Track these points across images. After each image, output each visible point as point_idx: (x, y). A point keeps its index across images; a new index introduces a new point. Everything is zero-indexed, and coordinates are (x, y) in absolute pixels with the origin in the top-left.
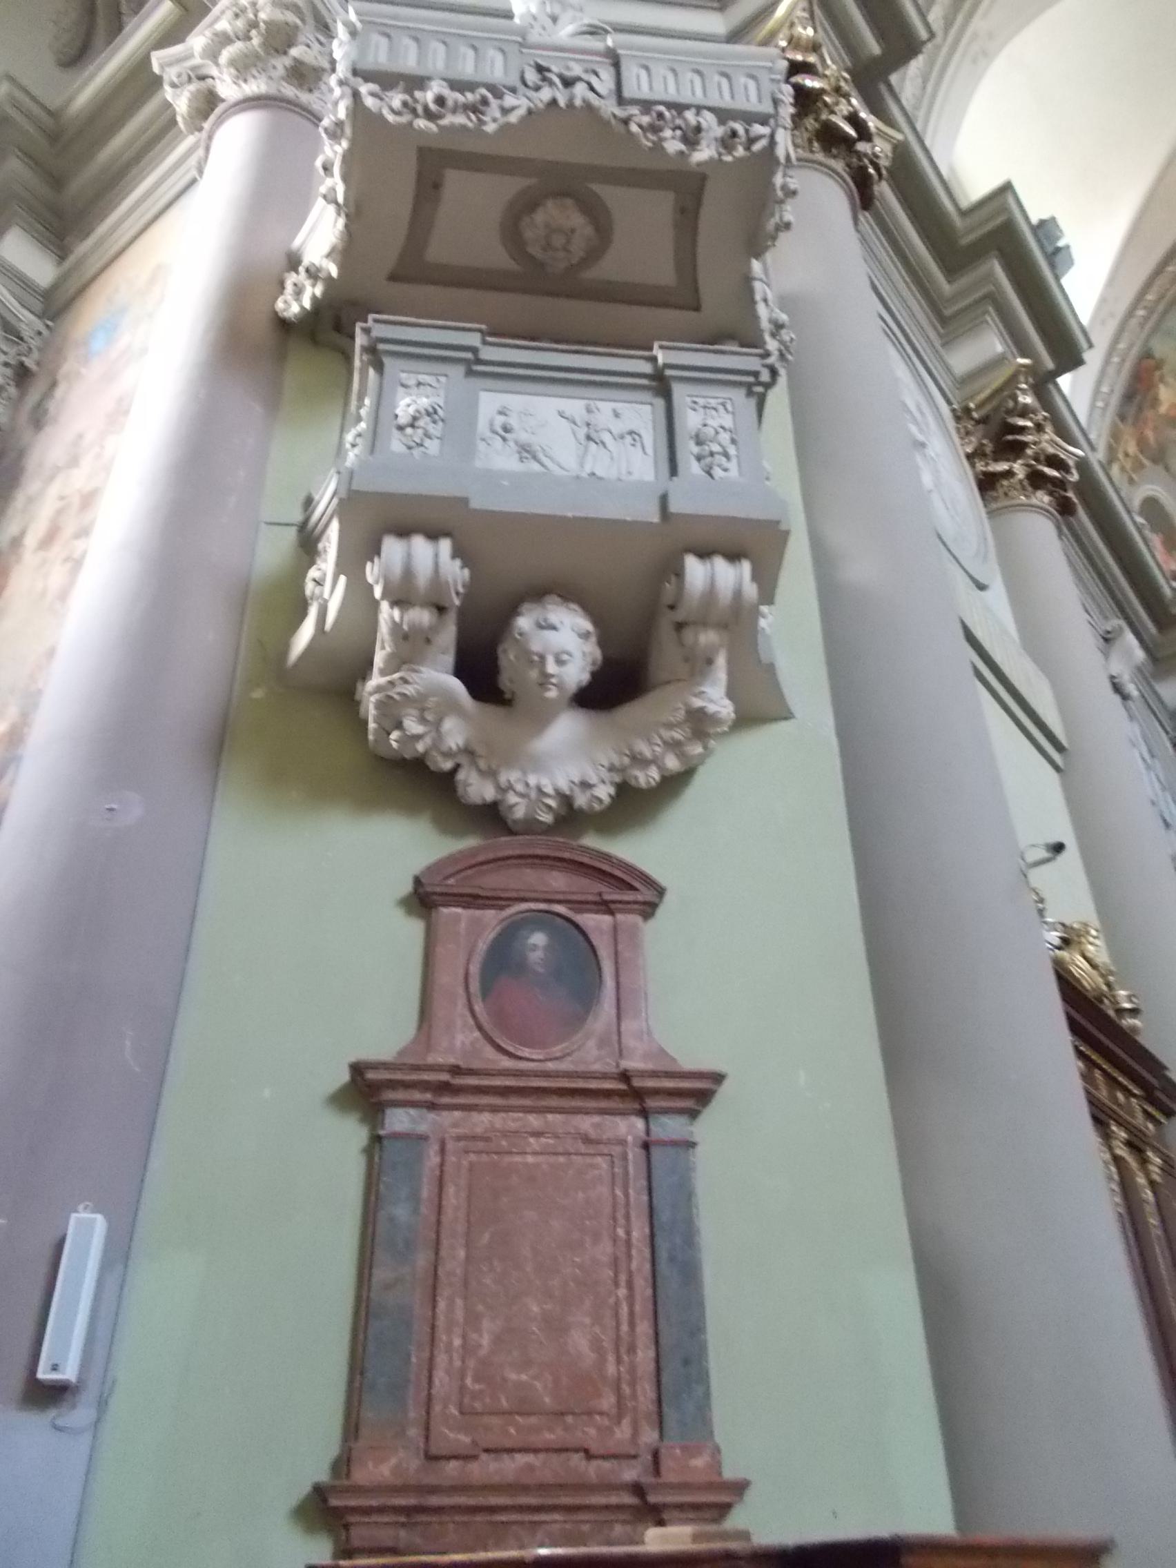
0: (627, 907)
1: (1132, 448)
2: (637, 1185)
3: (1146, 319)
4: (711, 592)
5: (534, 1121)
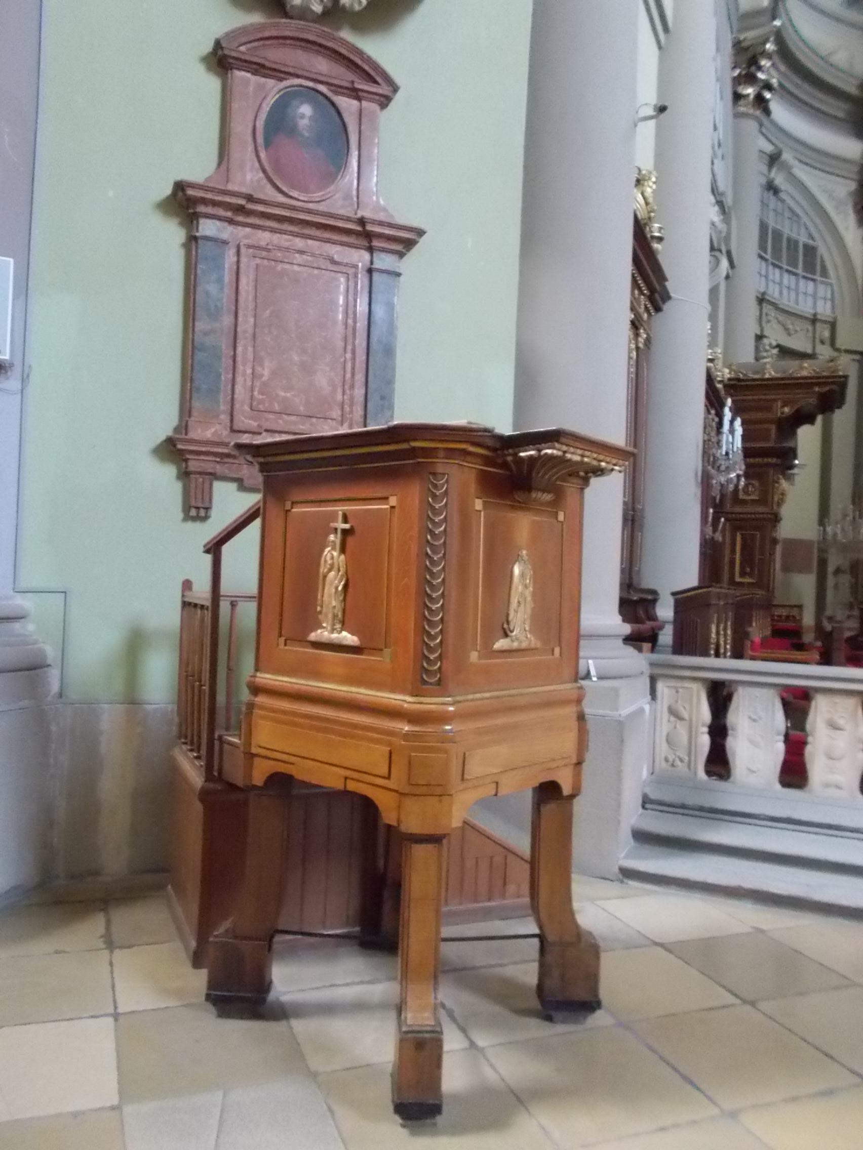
5: (299, 243)
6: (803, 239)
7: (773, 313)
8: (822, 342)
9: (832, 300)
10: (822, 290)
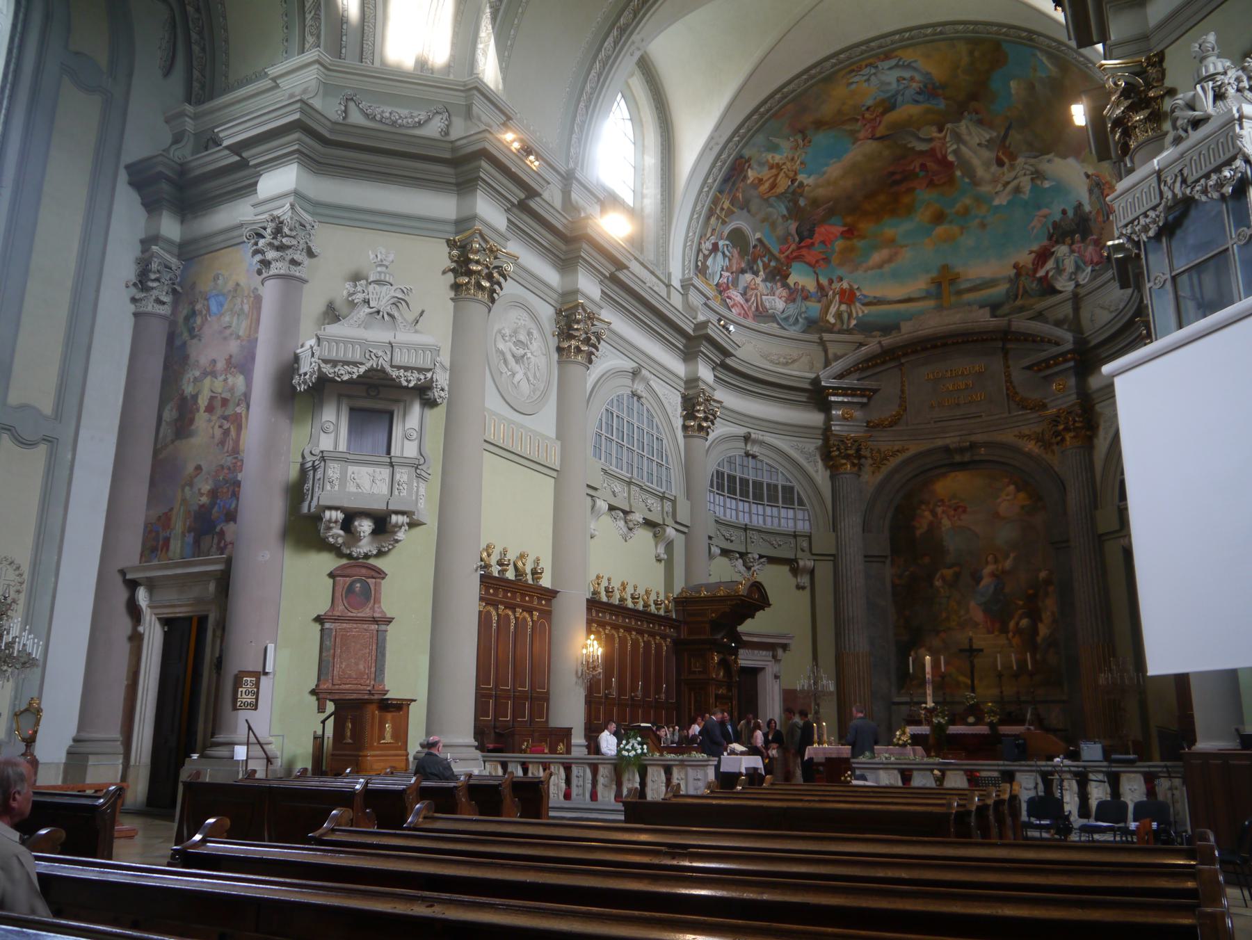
0: (379, 578)
1: (727, 205)
2: (375, 638)
3: (739, 142)
4: (397, 523)
5: (355, 625)
6: (781, 482)
7: (755, 536)
8: (803, 550)
9: (809, 520)
10: (800, 515)
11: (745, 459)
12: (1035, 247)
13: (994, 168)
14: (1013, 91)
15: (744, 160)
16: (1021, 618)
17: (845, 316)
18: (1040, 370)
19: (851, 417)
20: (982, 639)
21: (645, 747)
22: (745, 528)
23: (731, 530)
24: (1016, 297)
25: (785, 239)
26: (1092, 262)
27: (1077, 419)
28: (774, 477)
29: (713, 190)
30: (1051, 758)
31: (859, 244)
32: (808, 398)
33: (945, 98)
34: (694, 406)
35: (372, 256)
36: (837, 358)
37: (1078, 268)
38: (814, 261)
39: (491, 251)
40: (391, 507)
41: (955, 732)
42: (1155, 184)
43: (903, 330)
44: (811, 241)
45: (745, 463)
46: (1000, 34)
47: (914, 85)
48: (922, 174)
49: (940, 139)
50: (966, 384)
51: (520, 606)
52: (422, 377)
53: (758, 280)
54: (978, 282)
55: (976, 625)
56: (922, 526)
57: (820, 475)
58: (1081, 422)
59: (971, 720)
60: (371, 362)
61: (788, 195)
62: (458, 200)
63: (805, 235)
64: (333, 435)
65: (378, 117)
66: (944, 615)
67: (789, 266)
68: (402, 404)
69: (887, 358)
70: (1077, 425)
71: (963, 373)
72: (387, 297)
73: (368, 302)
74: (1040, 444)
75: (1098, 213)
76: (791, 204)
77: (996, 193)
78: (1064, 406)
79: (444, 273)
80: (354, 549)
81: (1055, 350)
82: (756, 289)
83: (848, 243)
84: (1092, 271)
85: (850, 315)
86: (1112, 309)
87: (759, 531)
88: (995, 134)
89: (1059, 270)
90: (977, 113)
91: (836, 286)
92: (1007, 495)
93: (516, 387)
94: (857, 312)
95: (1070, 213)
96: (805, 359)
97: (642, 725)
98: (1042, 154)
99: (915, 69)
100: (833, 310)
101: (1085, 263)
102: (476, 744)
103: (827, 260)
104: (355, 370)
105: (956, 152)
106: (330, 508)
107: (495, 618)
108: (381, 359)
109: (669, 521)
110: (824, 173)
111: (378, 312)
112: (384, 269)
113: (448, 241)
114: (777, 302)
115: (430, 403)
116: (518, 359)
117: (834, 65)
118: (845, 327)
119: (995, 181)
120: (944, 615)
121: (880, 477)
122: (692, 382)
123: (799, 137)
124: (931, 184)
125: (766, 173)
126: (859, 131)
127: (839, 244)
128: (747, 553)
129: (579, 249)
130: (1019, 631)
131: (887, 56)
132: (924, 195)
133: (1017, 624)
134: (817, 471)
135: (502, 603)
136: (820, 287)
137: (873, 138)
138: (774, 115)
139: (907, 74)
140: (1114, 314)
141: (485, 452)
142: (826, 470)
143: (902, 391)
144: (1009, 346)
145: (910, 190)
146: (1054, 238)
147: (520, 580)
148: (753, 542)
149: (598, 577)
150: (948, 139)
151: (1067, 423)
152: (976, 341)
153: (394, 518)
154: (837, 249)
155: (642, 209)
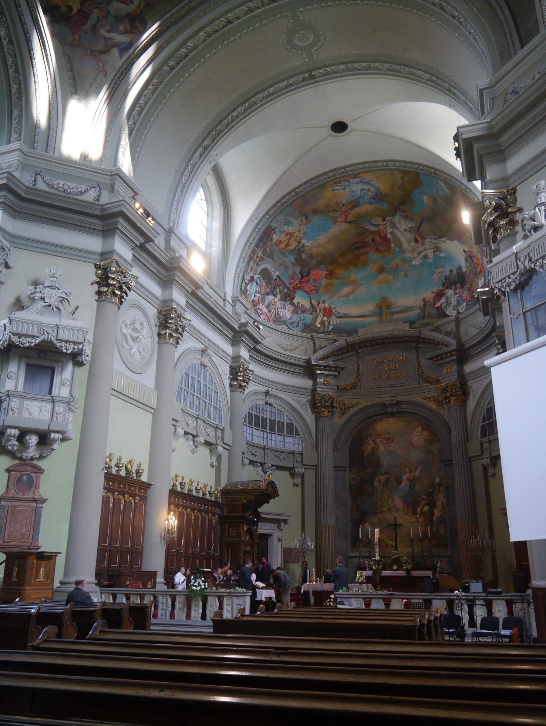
0: (39, 473)
1: (260, 254)
2: (34, 512)
4: (54, 438)
5: (21, 503)
6: (286, 420)
7: (270, 453)
8: (298, 462)
10: (297, 441)
11: (265, 406)
12: (435, 290)
13: (413, 244)
14: (425, 202)
15: (271, 229)
16: (424, 506)
17: (326, 323)
18: (437, 360)
19: (328, 383)
20: (402, 518)
21: (206, 584)
22: (264, 448)
23: (256, 449)
24: (424, 317)
25: (293, 277)
26: (466, 300)
27: (458, 390)
28: (282, 417)
29: (252, 245)
30: (452, 591)
31: (335, 282)
32: (304, 371)
33: (387, 203)
34: (237, 373)
35: (47, 271)
36: (321, 348)
37: (458, 303)
38: (309, 290)
39: (122, 273)
40: (51, 428)
41: (386, 575)
42: (514, 260)
43: (360, 334)
44: (308, 279)
45: (265, 409)
46: (419, 169)
47: (370, 194)
48: (372, 244)
49: (383, 225)
50: (395, 367)
51: (128, 493)
52: (76, 347)
53: (277, 300)
54: (403, 308)
55: (398, 510)
56: (368, 450)
57: (309, 417)
58: (460, 391)
59: (395, 567)
60: (44, 336)
61: (296, 251)
62: (103, 240)
63: (305, 275)
64: (14, 381)
65: (55, 186)
66: (380, 503)
67: (295, 292)
68: (61, 364)
69: (350, 349)
70: (458, 393)
71: (393, 360)
72: (56, 297)
73: (44, 299)
74: (436, 403)
75: (470, 273)
76: (297, 256)
77: (414, 258)
78: (450, 382)
79: (92, 284)
80: (24, 454)
81: (446, 349)
82: (275, 305)
83: (329, 281)
84: (466, 305)
85: (329, 323)
86: (477, 327)
87: (272, 450)
88: (414, 225)
89: (448, 304)
90: (404, 212)
91: (322, 305)
92: (418, 432)
93: (132, 356)
94: (333, 322)
95: (455, 272)
96: (302, 348)
97: (205, 570)
98: (440, 238)
99: (371, 185)
100: (319, 319)
101: (463, 301)
102: (96, 582)
103: (317, 290)
104: (33, 340)
105: (392, 233)
106: (11, 427)
107: (112, 500)
108: (50, 335)
109: (220, 442)
110: (317, 240)
111: (50, 306)
112: (55, 279)
113: (95, 265)
114: (287, 313)
115: (80, 364)
116: (134, 339)
117: (325, 179)
118: (326, 330)
119: (413, 251)
120: (380, 503)
121: (344, 419)
122: (236, 358)
123: (304, 219)
124: (377, 250)
125: (283, 238)
126: (338, 217)
127: (324, 281)
128: (265, 463)
129: (174, 275)
130: (422, 514)
131: (356, 176)
132: (373, 256)
133: (422, 509)
134: (307, 415)
135: (117, 491)
136: (312, 306)
137: (346, 222)
138: (290, 205)
139: (366, 187)
140: (479, 330)
141: (112, 396)
142: (313, 414)
143: (358, 369)
144: (420, 345)
145: (366, 253)
146: (446, 286)
147: (129, 476)
148: (268, 457)
149: (176, 476)
150: (388, 225)
151: (452, 391)
152: (402, 342)
153: (53, 435)
154: (323, 284)
155: (210, 253)
